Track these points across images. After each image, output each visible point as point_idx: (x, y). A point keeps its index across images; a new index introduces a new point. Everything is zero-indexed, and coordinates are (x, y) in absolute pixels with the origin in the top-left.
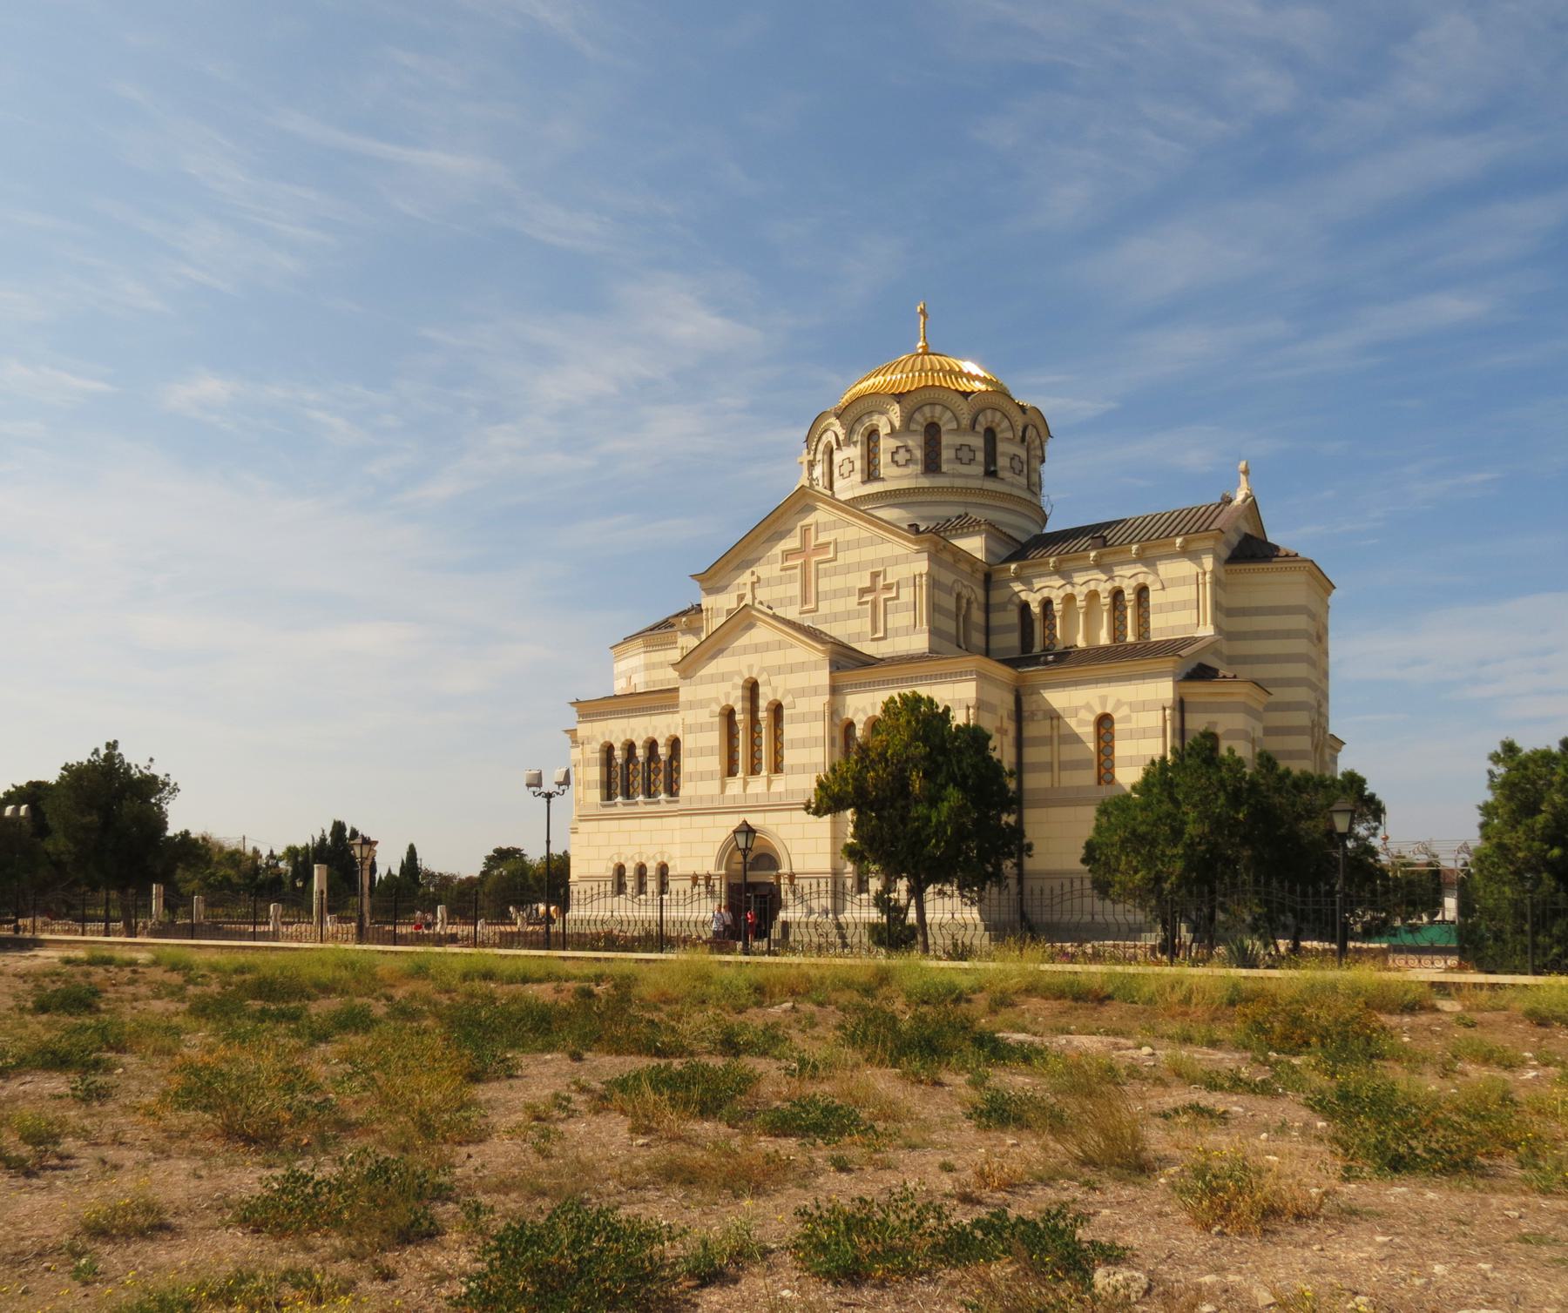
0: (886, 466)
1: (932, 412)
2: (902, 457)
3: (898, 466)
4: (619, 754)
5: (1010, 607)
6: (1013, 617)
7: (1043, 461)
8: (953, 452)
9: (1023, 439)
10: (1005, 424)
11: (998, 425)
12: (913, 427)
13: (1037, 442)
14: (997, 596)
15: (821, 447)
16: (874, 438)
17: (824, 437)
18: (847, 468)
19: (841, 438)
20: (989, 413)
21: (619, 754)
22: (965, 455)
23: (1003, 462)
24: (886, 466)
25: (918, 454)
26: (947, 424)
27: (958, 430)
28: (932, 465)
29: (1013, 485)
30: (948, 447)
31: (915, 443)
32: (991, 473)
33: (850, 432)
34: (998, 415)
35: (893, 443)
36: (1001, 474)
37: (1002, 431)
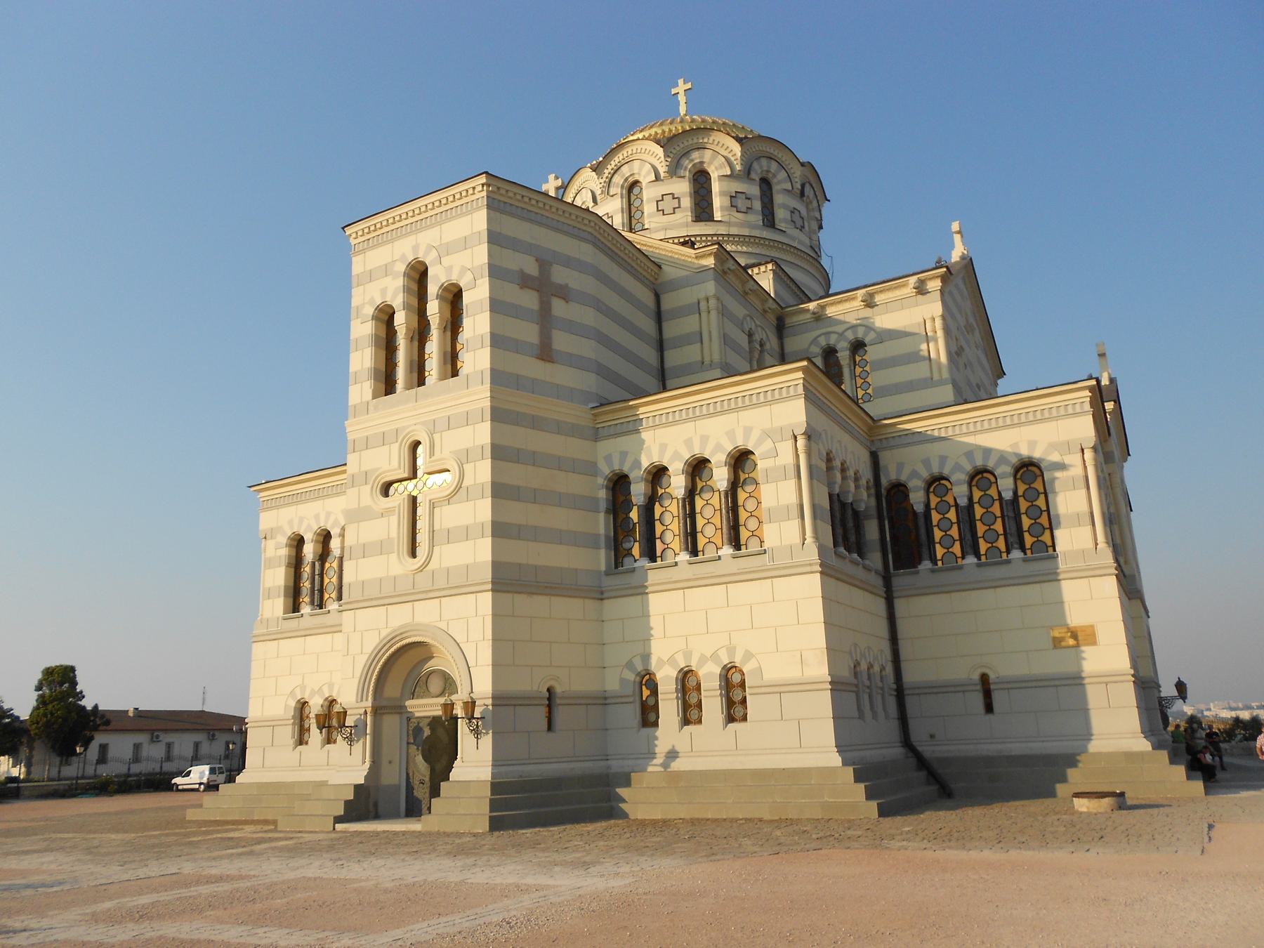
2: (668, 204)
3: (664, 215)
4: (309, 551)
7: (821, 227)
8: (729, 198)
9: (802, 194)
10: (782, 175)
11: (774, 176)
12: (682, 173)
13: (815, 204)
16: (636, 190)
19: (598, 192)
20: (764, 162)
21: (309, 551)
22: (741, 203)
23: (781, 214)
24: (650, 215)
25: (687, 202)
26: (716, 171)
27: (733, 176)
29: (793, 239)
30: (722, 194)
31: (682, 187)
32: (769, 220)
34: (774, 166)
37: (779, 182)
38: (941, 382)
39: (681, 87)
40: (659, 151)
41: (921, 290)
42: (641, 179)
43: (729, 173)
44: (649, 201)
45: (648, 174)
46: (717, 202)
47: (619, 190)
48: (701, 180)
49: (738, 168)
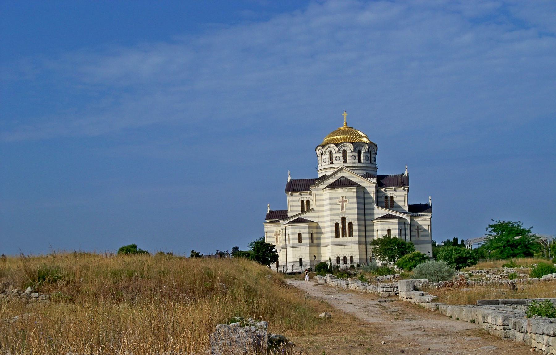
0: (349, 160)
1: (360, 148)
2: (353, 158)
5: (382, 197)
6: (383, 199)
10: (373, 150)
14: (380, 194)
15: (327, 151)
17: (329, 148)
18: (338, 159)
22: (367, 158)
23: (373, 159)
24: (349, 160)
25: (357, 158)
26: (363, 151)
28: (360, 161)
30: (364, 156)
31: (356, 154)
33: (339, 150)
35: (351, 154)
36: (373, 162)
37: (372, 152)
38: (407, 207)
39: (345, 114)
40: (352, 146)
41: (404, 189)
42: (347, 150)
43: (365, 152)
44: (349, 156)
45: (349, 150)
46: (362, 158)
47: (342, 152)
48: (359, 153)
49: (367, 151)
